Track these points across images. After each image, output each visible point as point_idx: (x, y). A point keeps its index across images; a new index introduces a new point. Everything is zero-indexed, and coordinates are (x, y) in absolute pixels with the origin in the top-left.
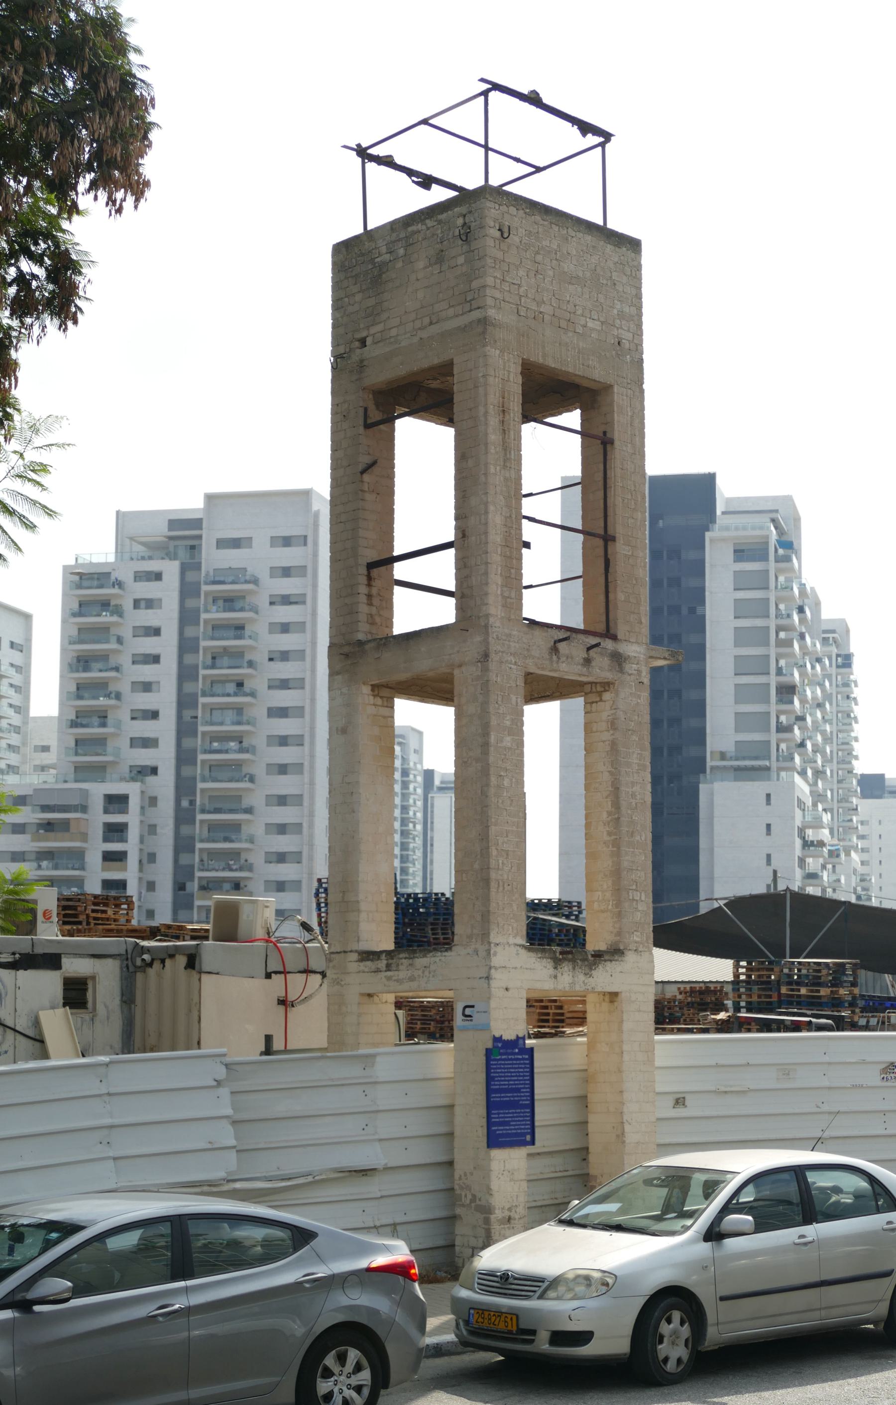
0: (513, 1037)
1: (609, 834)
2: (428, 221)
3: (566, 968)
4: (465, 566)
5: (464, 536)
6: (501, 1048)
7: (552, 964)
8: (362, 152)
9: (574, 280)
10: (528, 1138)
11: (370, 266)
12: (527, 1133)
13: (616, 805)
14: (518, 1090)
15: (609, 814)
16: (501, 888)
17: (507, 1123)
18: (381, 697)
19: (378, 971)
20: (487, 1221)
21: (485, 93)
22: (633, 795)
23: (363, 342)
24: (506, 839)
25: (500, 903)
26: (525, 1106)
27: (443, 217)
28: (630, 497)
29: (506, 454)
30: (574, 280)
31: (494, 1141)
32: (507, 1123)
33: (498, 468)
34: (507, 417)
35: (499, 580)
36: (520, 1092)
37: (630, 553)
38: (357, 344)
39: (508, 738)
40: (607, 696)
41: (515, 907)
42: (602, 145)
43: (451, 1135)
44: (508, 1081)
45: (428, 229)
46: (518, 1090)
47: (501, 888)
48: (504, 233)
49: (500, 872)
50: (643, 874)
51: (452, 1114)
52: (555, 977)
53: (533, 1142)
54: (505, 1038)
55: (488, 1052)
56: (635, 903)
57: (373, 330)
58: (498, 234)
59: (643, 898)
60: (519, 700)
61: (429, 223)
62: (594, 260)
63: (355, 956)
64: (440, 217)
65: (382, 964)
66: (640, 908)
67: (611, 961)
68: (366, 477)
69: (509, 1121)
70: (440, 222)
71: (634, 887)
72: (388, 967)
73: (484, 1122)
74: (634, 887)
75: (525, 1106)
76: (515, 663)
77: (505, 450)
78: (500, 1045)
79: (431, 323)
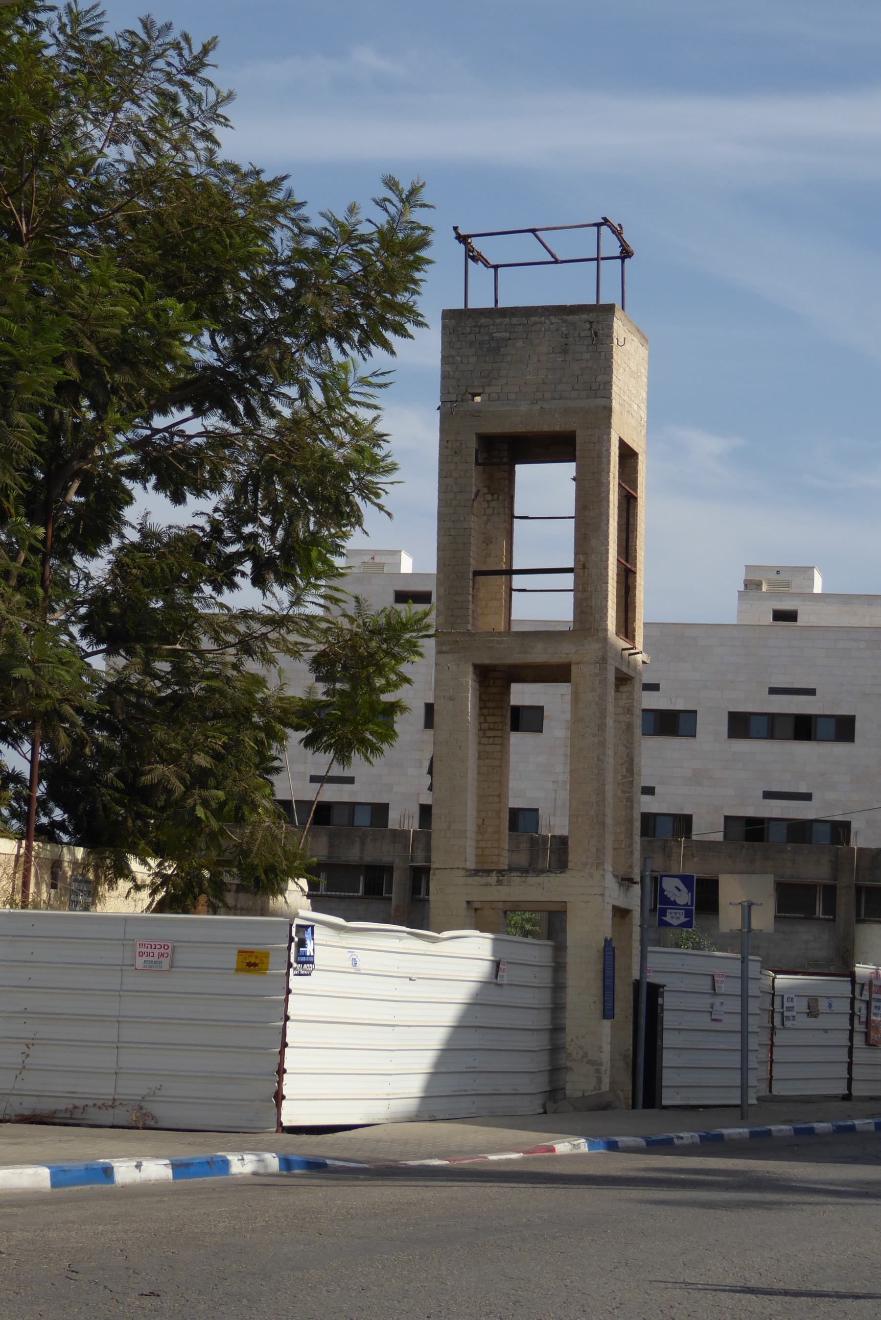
1: (624, 792)
2: (551, 318)
4: (585, 590)
5: (584, 567)
11: (487, 338)
15: (624, 777)
19: (486, 885)
20: (598, 1071)
21: (598, 225)
27: (570, 318)
38: (470, 397)
45: (552, 324)
57: (488, 390)
61: (554, 319)
64: (565, 317)
65: (493, 879)
70: (565, 321)
72: (499, 883)
79: (553, 399)
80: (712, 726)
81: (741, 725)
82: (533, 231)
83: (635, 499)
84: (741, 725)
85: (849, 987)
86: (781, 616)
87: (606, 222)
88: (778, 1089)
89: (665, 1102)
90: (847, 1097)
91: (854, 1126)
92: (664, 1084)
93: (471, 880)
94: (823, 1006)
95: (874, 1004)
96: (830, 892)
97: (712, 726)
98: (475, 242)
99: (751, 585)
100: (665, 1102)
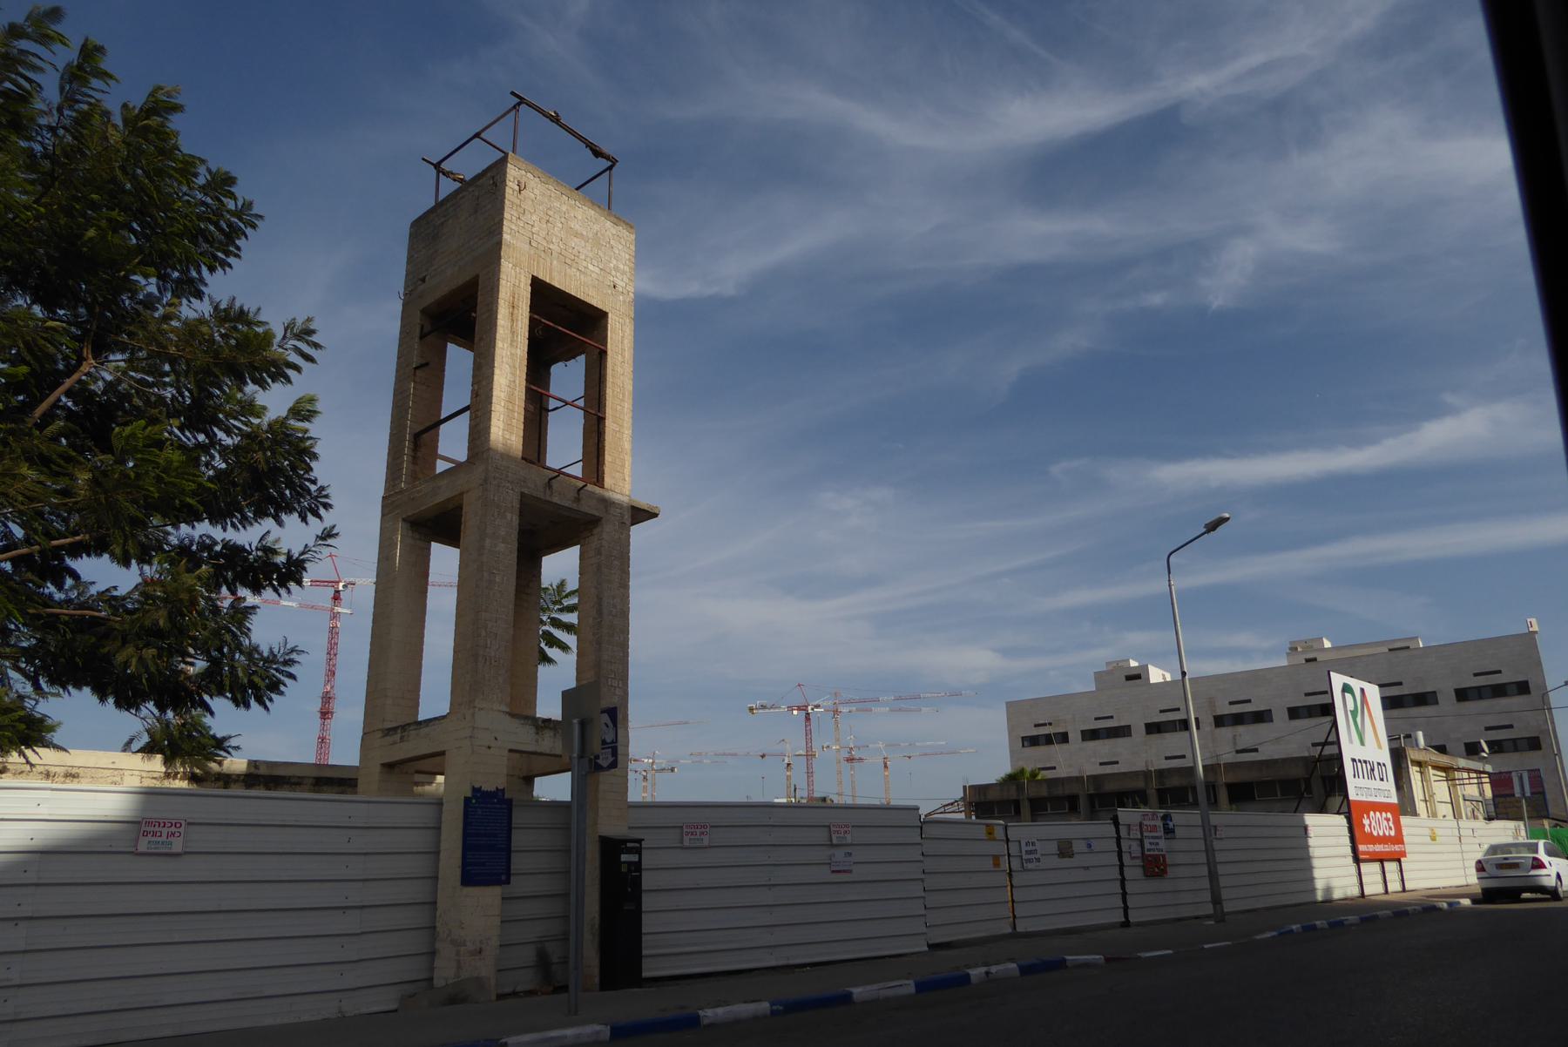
0: (493, 789)
8: (437, 166)
9: (577, 235)
13: (600, 612)
19: (395, 743)
23: (423, 280)
30: (577, 235)
31: (468, 879)
35: (501, 425)
40: (596, 531)
42: (610, 168)
43: (436, 878)
48: (521, 188)
51: (437, 861)
53: (508, 882)
54: (485, 788)
55: (467, 800)
62: (596, 227)
63: (380, 734)
65: (397, 737)
68: (419, 372)
73: (459, 862)
77: (513, 333)
80: (1280, 716)
81: (1294, 713)
82: (477, 135)
83: (605, 352)
84: (1294, 713)
85: (1113, 828)
86: (1308, 661)
87: (522, 101)
88: (1021, 927)
89: (645, 974)
90: (1126, 924)
91: (850, 995)
92: (644, 952)
93: (389, 739)
94: (1078, 846)
95: (1146, 842)
96: (1308, 781)
97: (1280, 716)
98: (445, 166)
99: (1294, 649)
100: (645, 974)
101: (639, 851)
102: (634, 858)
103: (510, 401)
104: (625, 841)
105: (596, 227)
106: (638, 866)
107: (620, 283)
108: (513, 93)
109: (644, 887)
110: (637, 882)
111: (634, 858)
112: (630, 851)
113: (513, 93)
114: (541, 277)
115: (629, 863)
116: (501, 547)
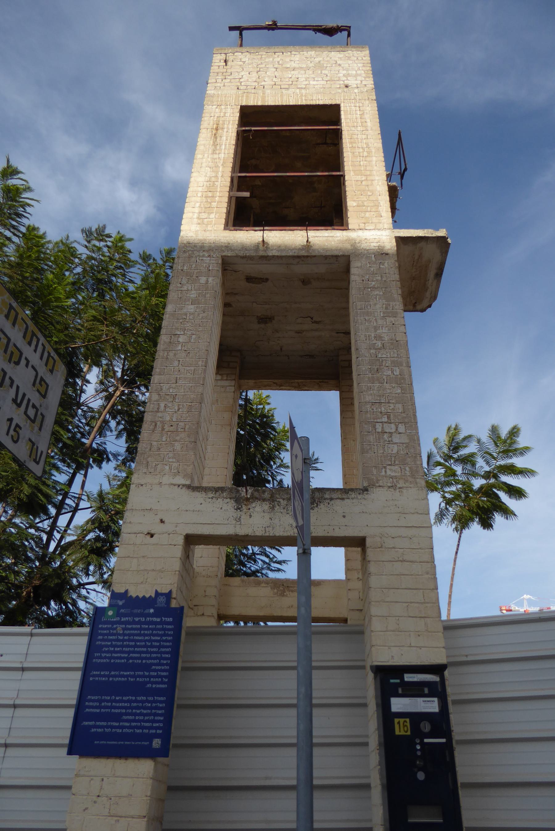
3: (258, 509)
6: (123, 607)
7: (232, 503)
10: (157, 743)
12: (156, 736)
14: (148, 667)
16: (159, 429)
17: (117, 718)
18: (220, 375)
22: (379, 337)
24: (174, 385)
25: (154, 443)
26: (159, 692)
28: (361, 150)
29: (216, 147)
32: (117, 718)
33: (206, 155)
34: (220, 131)
36: (150, 670)
37: (363, 179)
39: (192, 307)
41: (178, 446)
44: (129, 652)
46: (148, 667)
47: (159, 429)
49: (160, 414)
50: (400, 406)
52: (238, 520)
54: (133, 593)
56: (386, 436)
58: (225, 64)
59: (401, 428)
60: (210, 279)
66: (396, 439)
67: (343, 499)
69: (121, 714)
71: (385, 419)
74: (385, 419)
75: (159, 692)
76: (209, 256)
77: (215, 144)
78: (120, 603)
101: (438, 691)
102: (431, 705)
103: (211, 188)
104: (399, 671)
105: (317, 60)
106: (440, 723)
107: (352, 82)
108: (231, 29)
109: (461, 779)
110: (442, 761)
111: (431, 705)
112: (415, 690)
113: (231, 29)
114: (251, 103)
115: (416, 718)
116: (191, 308)
